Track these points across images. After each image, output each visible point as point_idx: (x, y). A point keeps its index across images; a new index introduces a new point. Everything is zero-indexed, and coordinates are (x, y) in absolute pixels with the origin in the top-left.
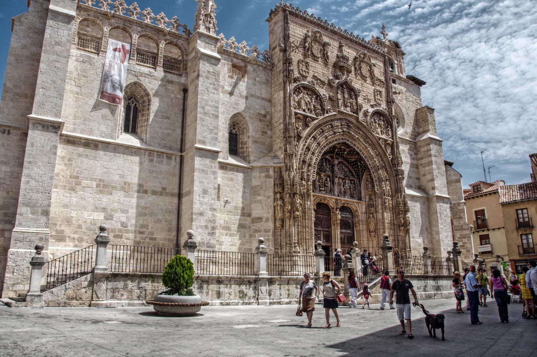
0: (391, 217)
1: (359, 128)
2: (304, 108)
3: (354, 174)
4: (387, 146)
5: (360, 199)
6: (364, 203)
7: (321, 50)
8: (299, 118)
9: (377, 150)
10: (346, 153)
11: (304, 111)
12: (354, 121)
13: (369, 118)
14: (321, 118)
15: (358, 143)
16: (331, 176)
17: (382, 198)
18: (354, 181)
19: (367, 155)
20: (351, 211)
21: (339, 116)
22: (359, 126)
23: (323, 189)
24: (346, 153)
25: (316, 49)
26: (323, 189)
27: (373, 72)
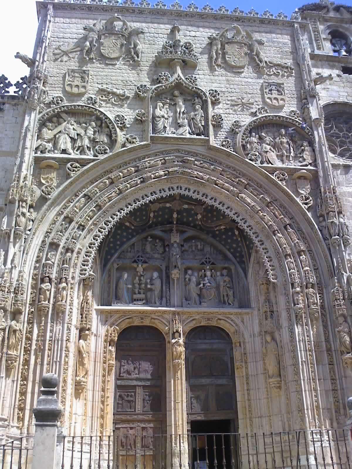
0: (317, 335)
1: (213, 161)
2: (63, 147)
3: (230, 256)
4: (300, 182)
5: (244, 304)
6: (256, 312)
7: (122, 45)
8: (50, 167)
9: (267, 192)
10: (199, 217)
11: (64, 151)
12: (201, 150)
13: (239, 136)
14: (101, 157)
15: (213, 189)
16: (164, 268)
17: (287, 295)
18: (229, 270)
19: (238, 209)
20: (228, 335)
21: (160, 147)
22: (213, 157)
23: (142, 296)
24: (199, 217)
25: (110, 47)
26: (142, 296)
27: (258, 55)
